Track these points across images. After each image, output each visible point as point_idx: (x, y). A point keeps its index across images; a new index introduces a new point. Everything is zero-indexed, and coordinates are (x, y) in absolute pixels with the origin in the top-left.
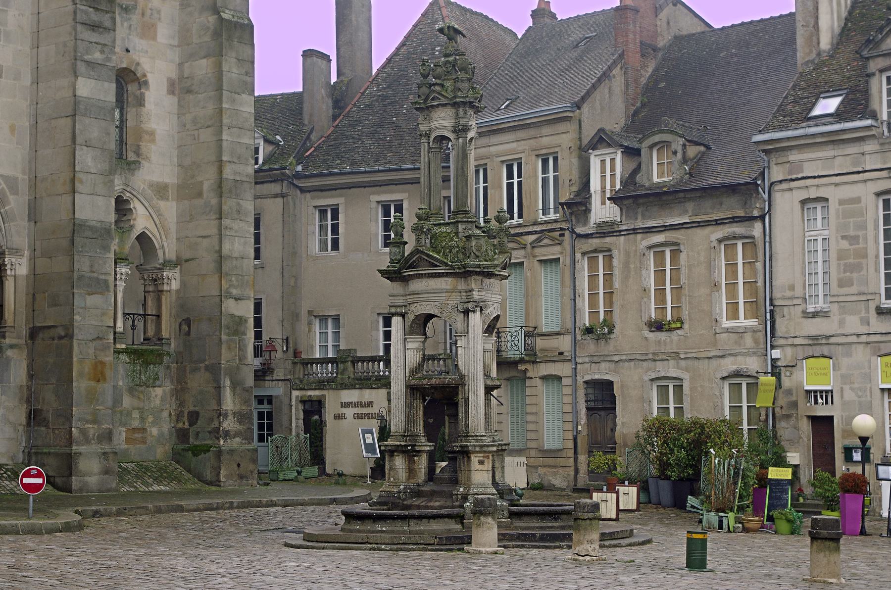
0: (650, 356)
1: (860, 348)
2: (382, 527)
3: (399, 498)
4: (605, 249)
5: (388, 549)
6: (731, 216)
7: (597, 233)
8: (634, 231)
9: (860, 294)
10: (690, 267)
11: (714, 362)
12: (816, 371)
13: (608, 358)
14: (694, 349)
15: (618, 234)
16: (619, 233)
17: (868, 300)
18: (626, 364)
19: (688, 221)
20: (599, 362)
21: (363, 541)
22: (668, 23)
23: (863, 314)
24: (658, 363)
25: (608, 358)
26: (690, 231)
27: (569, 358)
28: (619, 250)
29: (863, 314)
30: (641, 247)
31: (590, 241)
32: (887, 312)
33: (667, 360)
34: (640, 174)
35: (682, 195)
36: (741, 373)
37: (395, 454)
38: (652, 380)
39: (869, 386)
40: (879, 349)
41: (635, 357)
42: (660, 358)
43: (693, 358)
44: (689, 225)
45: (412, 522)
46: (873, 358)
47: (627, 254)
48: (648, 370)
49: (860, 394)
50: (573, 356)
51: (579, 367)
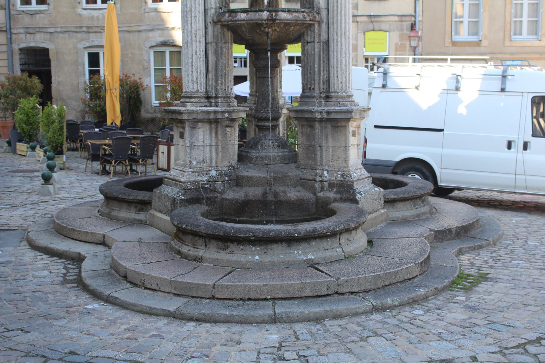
0: (85, 29)
2: (305, 253)
3: (215, 190)
5: (396, 303)
11: (144, 35)
13: (44, 30)
14: (125, 24)
18: (61, 35)
20: (34, 33)
24: (91, 35)
25: (44, 30)
27: (5, 29)
33: (101, 32)
36: (168, 43)
37: (200, 124)
38: (85, 48)
41: (69, 29)
42: (94, 30)
48: (82, 40)
50: (8, 27)
51: (14, 36)
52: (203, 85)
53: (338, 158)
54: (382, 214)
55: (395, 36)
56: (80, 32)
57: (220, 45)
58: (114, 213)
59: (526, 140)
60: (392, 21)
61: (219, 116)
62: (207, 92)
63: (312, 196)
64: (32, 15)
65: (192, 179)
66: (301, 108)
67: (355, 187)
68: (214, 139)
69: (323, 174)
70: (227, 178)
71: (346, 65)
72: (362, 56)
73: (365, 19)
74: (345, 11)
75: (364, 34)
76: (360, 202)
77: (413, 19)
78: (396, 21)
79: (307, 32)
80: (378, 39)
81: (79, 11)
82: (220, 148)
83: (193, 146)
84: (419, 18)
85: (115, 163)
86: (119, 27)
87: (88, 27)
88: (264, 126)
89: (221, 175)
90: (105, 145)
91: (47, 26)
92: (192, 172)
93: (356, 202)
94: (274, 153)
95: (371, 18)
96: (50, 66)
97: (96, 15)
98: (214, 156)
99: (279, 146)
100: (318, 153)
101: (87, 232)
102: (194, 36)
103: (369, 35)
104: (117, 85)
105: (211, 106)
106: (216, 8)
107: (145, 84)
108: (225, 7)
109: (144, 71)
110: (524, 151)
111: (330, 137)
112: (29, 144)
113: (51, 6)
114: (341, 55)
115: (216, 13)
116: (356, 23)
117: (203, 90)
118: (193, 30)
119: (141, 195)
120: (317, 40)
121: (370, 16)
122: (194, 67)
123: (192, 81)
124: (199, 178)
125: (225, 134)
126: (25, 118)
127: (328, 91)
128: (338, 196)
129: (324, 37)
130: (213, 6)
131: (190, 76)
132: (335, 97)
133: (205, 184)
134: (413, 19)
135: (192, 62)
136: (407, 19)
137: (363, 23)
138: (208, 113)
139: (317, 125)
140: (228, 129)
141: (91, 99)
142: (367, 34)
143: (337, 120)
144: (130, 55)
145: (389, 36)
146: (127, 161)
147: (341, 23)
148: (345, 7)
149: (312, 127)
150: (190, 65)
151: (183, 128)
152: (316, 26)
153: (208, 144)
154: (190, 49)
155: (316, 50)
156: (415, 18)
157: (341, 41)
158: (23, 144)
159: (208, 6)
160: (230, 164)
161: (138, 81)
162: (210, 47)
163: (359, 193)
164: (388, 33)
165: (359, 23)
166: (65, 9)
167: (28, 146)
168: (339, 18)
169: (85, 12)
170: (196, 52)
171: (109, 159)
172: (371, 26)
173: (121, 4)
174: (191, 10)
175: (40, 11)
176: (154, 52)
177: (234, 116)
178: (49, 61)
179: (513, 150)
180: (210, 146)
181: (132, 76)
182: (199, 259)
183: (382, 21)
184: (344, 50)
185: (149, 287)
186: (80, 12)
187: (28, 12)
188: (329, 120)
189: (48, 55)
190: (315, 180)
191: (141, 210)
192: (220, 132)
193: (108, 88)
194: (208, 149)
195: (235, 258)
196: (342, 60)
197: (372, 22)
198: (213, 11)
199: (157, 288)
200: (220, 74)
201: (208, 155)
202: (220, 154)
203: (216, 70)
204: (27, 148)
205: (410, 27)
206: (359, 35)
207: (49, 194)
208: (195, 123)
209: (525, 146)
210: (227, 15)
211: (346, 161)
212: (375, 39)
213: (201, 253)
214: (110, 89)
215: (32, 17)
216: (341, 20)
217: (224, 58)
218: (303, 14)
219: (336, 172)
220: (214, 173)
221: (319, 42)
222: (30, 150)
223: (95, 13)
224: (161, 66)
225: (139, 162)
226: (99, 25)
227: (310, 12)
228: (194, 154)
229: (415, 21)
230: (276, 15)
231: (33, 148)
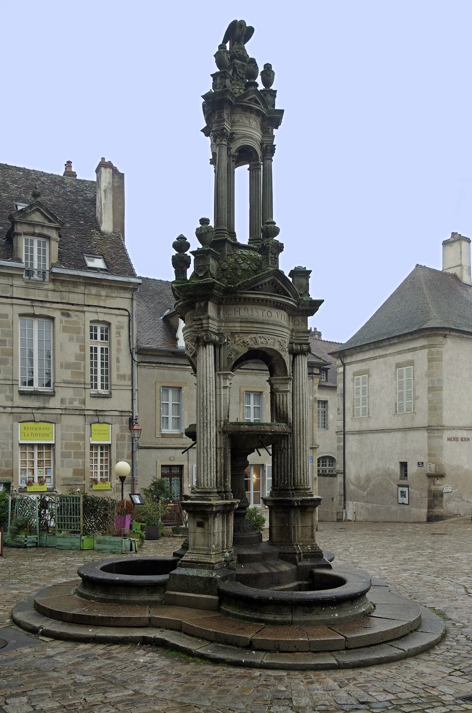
1: (5, 416)
9: (5, 379)
12: (99, 432)
17: (13, 384)
23: (8, 393)
29: (8, 393)
40: (20, 418)
46: (15, 424)
75: (91, 426)
77: (131, 414)
79: (281, 441)
84: (136, 414)
88: (239, 513)
111: (299, 519)
116: (84, 417)
118: (212, 438)
132: (303, 489)
134: (131, 414)
136: (127, 414)
142: (93, 425)
145: (112, 428)
156: (133, 414)
172: (96, 419)
182: (289, 623)
195: (317, 618)
197: (97, 415)
205: (128, 420)
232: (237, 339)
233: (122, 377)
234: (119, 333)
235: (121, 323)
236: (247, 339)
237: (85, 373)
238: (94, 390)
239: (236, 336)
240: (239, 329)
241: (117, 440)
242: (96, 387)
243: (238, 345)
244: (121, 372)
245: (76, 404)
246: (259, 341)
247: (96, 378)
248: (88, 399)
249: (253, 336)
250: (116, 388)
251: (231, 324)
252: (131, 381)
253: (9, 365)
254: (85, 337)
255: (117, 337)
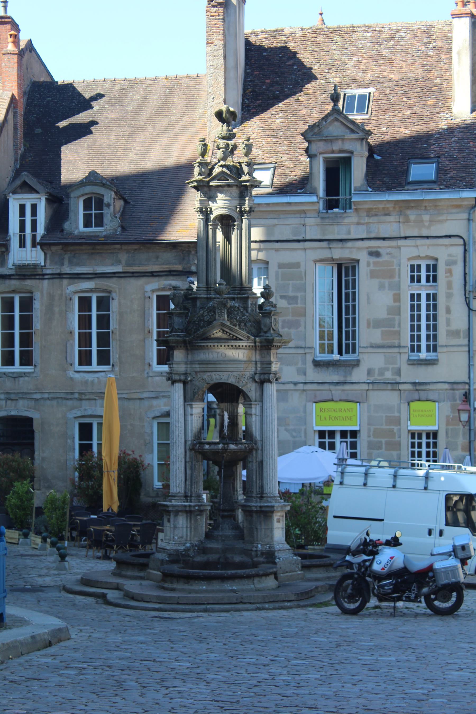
0: (77, 396)
1: (296, 395)
3: (189, 556)
4: (25, 291)
5: (271, 607)
6: (167, 270)
7: (17, 275)
8: (60, 276)
10: (121, 314)
11: (146, 403)
13: (28, 396)
14: (124, 390)
15: (41, 277)
16: (42, 277)
17: (305, 353)
18: (48, 402)
19: (121, 270)
20: (17, 400)
21: (237, 602)
22: (27, 68)
23: (300, 365)
24: (84, 402)
25: (28, 396)
26: (122, 280)
28: (42, 293)
29: (300, 365)
30: (68, 291)
31: (8, 282)
32: (324, 365)
33: (95, 399)
34: (68, 223)
35: (118, 246)
37: (180, 513)
38: (75, 418)
39: (303, 428)
40: (315, 396)
41: (58, 395)
42: (88, 397)
43: (125, 398)
44: (122, 275)
45: (256, 580)
46: (309, 404)
47: (51, 297)
48: (73, 408)
49: (294, 434)
52: (183, 488)
53: (268, 536)
54: (298, 574)
55: (446, 407)
56: (71, 399)
57: (194, 463)
58: (124, 573)
59: (442, 528)
60: (442, 390)
61: (192, 509)
62: (185, 492)
63: (250, 560)
64: (15, 378)
65: (174, 548)
66: (245, 504)
67: (276, 554)
68: (189, 523)
69: (258, 546)
70: (196, 548)
71: (272, 477)
72: (407, 431)
73: (409, 387)
74: (272, 442)
75: (409, 404)
76: (278, 564)
77: (467, 387)
78: (446, 389)
80: (425, 411)
81: (71, 374)
82: (193, 529)
83: (175, 527)
85: (117, 547)
86: (118, 394)
87: (80, 393)
89: (193, 546)
90: (108, 530)
91: (32, 392)
92: (175, 544)
93: (275, 563)
94: (229, 532)
95: (416, 386)
96: (33, 438)
97: (90, 379)
98: (189, 534)
99: (233, 529)
100: (255, 533)
101: (107, 582)
102: (177, 458)
103: (414, 405)
104: (116, 467)
105: (187, 502)
106: (191, 441)
107: (146, 462)
108: (198, 439)
109: (146, 446)
110: (440, 538)
112: (21, 531)
113: (38, 369)
114: (269, 470)
115: (191, 443)
116: (399, 392)
117: (183, 492)
118: (177, 454)
119: (142, 560)
120: (255, 461)
121: (414, 384)
122: (177, 478)
123: (176, 486)
124: (179, 548)
125: (196, 520)
126: (19, 503)
127: (262, 493)
128: (265, 560)
129: (259, 459)
130: (190, 439)
131: (175, 483)
133: (182, 552)
134: (467, 387)
135: (176, 474)
136: (460, 386)
137: (407, 392)
138: (185, 506)
139: (254, 515)
140: (199, 517)
141: (81, 478)
143: (266, 512)
144: (129, 427)
145: (438, 407)
146: (128, 546)
147: (269, 451)
148: (272, 441)
149: (251, 516)
150: (175, 476)
151: (170, 516)
152: (254, 452)
153: (185, 526)
154: (175, 466)
155: (254, 467)
156: (470, 386)
157: (269, 462)
158: (13, 531)
159: (187, 439)
160: (199, 539)
161: (138, 458)
162: (188, 464)
163: (279, 559)
164: (437, 403)
165: (402, 392)
166: (54, 371)
167: (21, 533)
168: (268, 447)
169: (77, 376)
170: (179, 468)
171: (111, 544)
172: (416, 396)
173: (120, 366)
174: (176, 442)
175: (25, 373)
176: (158, 423)
177: (202, 508)
178: (33, 432)
179: (432, 536)
180: (187, 527)
181: (130, 452)
183: (429, 390)
184: (271, 467)
185: (145, 600)
186: (72, 376)
187: (10, 375)
188: (262, 512)
189: (32, 425)
190: (252, 550)
191: (141, 570)
192: (193, 519)
193: (105, 469)
194: (185, 529)
196: (270, 474)
197: (417, 390)
198: (190, 442)
199: (149, 600)
200: (193, 482)
201: (185, 533)
202: (193, 533)
203: (191, 479)
204: (19, 535)
206: (402, 406)
207: (65, 569)
208: (177, 513)
209: (441, 533)
210: (198, 445)
211: (272, 538)
212: (422, 411)
213: (175, 586)
214: (108, 472)
215: (14, 380)
216: (269, 448)
217: (196, 471)
218: (245, 445)
219: (266, 545)
220: (188, 545)
221: (256, 462)
222: (23, 537)
223: (89, 377)
224: (166, 441)
225: (138, 548)
226: (93, 391)
227: (250, 443)
228: (176, 532)
229: (469, 390)
230: (228, 447)
231: (26, 536)
232: (199, 376)
233: (456, 334)
234: (449, 272)
235: (453, 256)
236: (206, 376)
237: (400, 331)
238: (416, 353)
239: (198, 374)
240: (198, 369)
241: (448, 424)
242: (419, 350)
243: (200, 381)
244: (454, 327)
245: (389, 375)
246: (214, 377)
247: (419, 337)
248: (405, 368)
249: (209, 374)
250: (445, 349)
251: (194, 366)
252: (467, 339)
253: (302, 329)
254: (400, 282)
255: (446, 277)
